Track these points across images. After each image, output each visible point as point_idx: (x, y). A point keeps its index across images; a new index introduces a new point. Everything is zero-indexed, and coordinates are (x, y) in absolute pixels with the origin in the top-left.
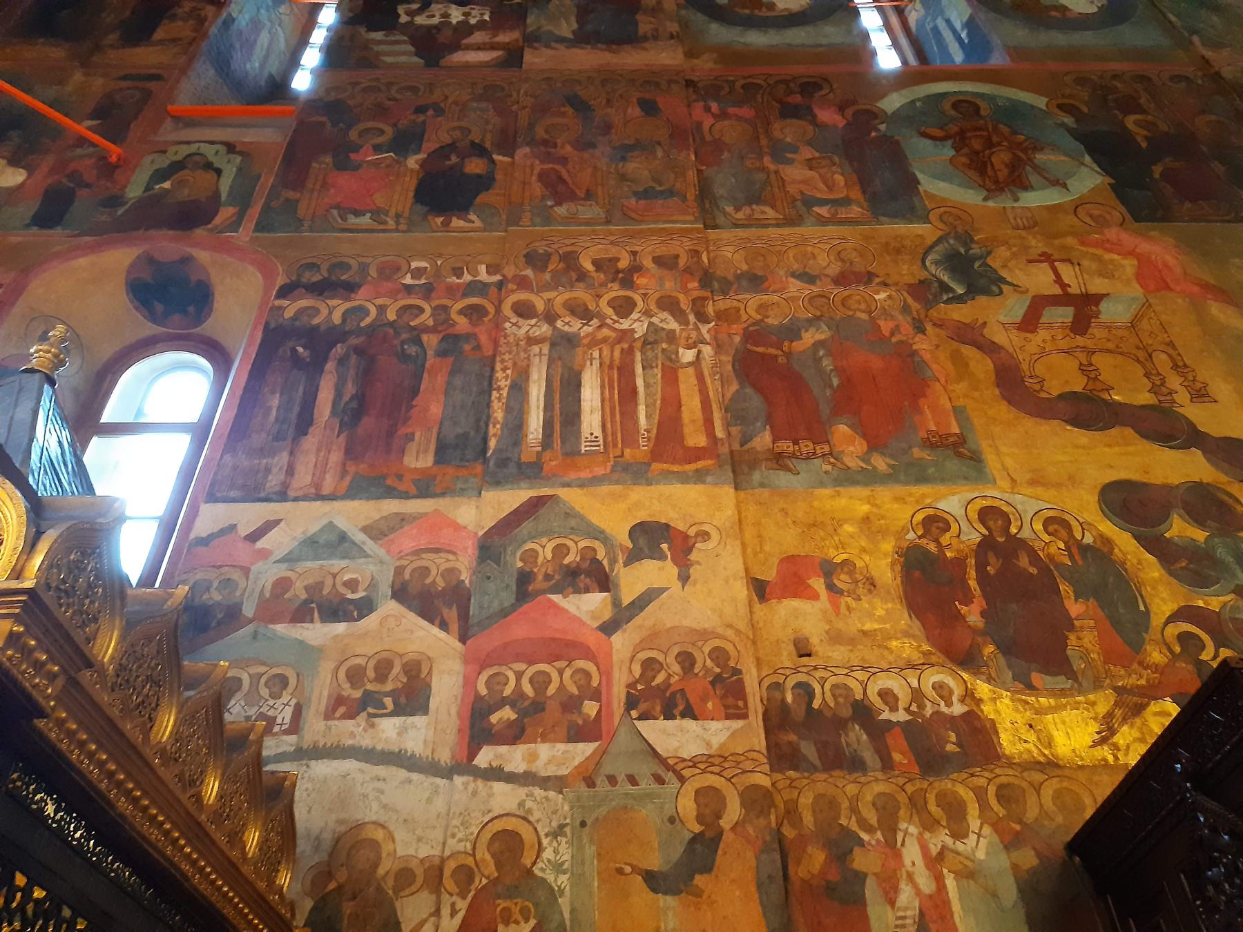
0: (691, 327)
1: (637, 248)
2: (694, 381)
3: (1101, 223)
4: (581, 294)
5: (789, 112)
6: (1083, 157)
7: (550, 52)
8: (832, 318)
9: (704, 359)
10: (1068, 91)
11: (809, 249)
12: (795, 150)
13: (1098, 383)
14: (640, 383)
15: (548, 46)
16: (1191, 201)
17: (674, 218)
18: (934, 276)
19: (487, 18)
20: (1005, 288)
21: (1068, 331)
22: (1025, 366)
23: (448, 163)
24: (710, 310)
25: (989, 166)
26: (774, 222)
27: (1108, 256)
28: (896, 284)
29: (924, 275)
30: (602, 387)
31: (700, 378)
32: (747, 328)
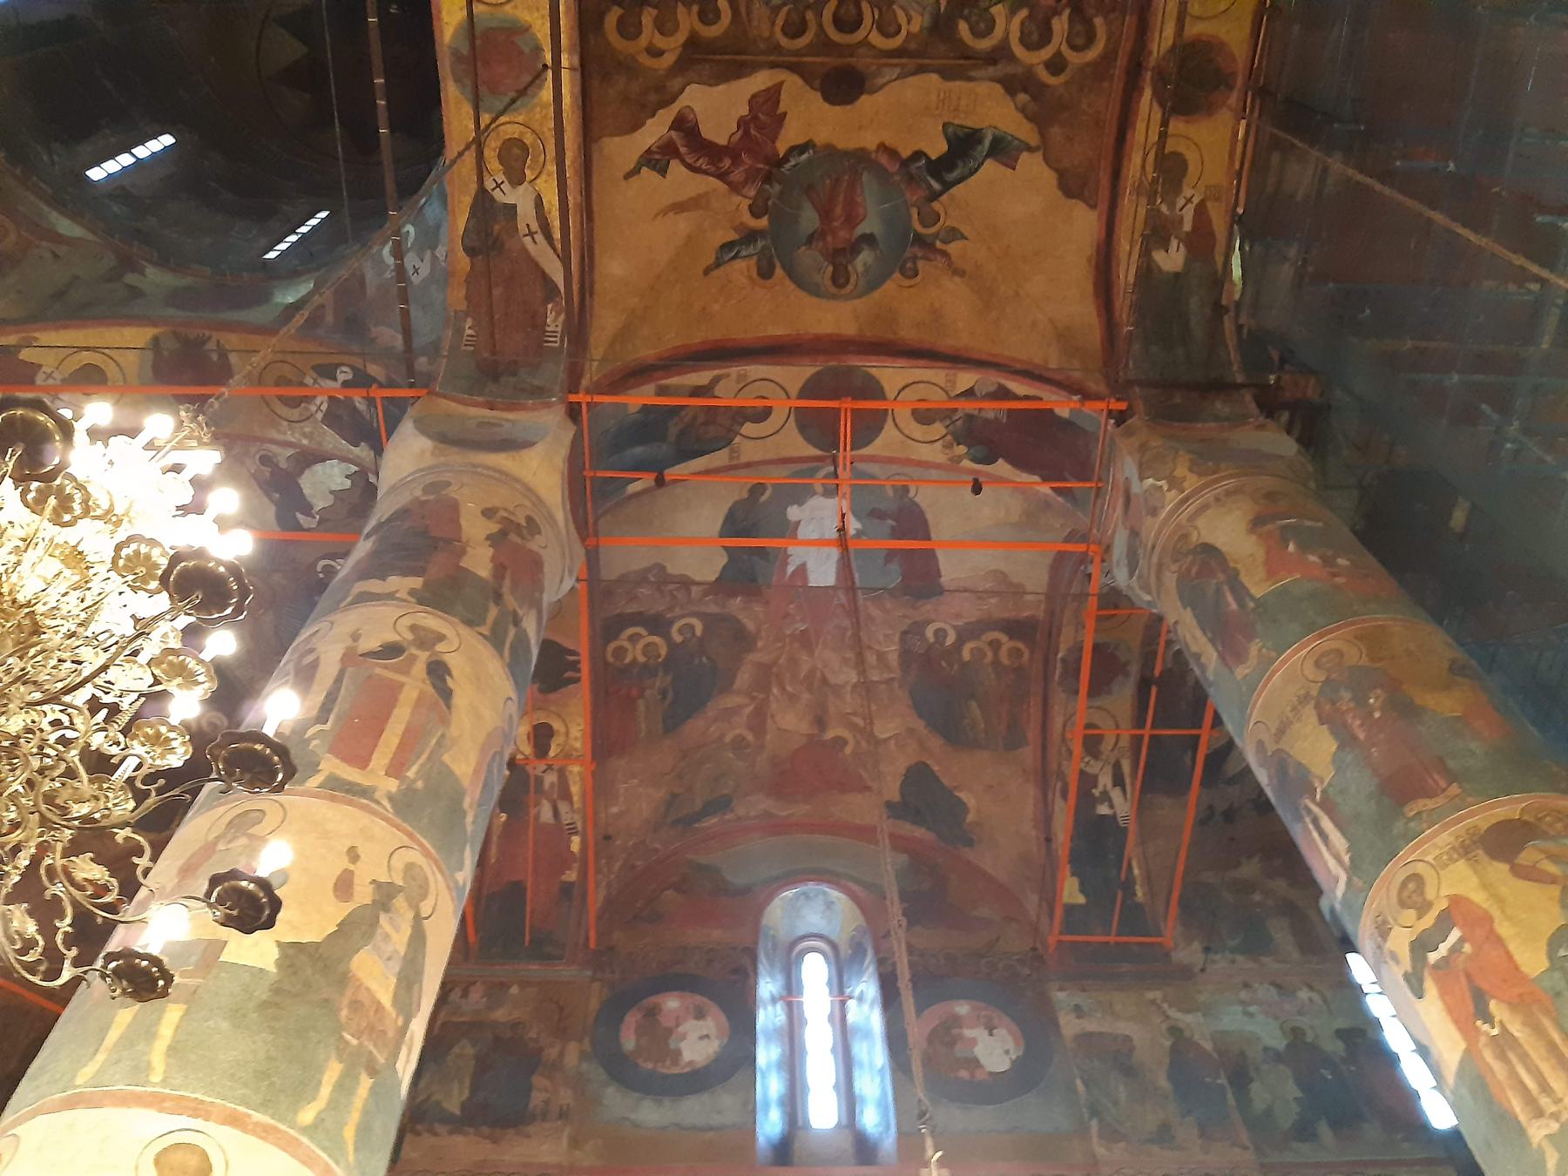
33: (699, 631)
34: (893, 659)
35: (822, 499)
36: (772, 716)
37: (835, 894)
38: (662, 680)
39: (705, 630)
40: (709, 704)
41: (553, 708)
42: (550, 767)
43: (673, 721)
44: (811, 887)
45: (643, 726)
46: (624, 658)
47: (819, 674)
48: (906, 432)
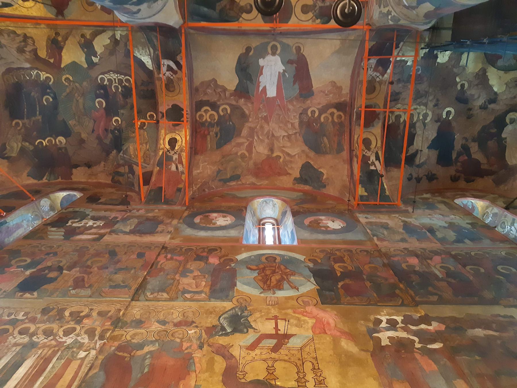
0: (93, 342)
1: (94, 308)
2: (77, 367)
3: (306, 304)
4: (55, 326)
5: (199, 258)
6: (311, 278)
7: (116, 236)
8: (163, 341)
9: (89, 356)
10: (315, 254)
11: (172, 311)
12: (192, 272)
13: (272, 375)
14: (51, 365)
15: (117, 234)
16: (350, 297)
17: (120, 296)
18: (221, 324)
19: (101, 225)
20: (250, 330)
21: (269, 351)
22: (241, 366)
23: (43, 273)
24: (108, 335)
25: (269, 280)
26: (164, 299)
27: (303, 318)
28: (202, 327)
29: (217, 323)
30: (31, 367)
31: (80, 366)
32: (121, 344)
33: (229, 112)
34: (297, 125)
35: (271, 56)
36: (255, 147)
37: (276, 201)
38: (216, 129)
39: (231, 110)
40: (232, 140)
41: (177, 132)
42: (175, 153)
43: (219, 146)
44: (267, 199)
45: (209, 146)
46: (203, 119)
47: (271, 133)
48: (299, 18)
